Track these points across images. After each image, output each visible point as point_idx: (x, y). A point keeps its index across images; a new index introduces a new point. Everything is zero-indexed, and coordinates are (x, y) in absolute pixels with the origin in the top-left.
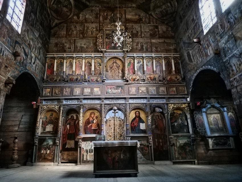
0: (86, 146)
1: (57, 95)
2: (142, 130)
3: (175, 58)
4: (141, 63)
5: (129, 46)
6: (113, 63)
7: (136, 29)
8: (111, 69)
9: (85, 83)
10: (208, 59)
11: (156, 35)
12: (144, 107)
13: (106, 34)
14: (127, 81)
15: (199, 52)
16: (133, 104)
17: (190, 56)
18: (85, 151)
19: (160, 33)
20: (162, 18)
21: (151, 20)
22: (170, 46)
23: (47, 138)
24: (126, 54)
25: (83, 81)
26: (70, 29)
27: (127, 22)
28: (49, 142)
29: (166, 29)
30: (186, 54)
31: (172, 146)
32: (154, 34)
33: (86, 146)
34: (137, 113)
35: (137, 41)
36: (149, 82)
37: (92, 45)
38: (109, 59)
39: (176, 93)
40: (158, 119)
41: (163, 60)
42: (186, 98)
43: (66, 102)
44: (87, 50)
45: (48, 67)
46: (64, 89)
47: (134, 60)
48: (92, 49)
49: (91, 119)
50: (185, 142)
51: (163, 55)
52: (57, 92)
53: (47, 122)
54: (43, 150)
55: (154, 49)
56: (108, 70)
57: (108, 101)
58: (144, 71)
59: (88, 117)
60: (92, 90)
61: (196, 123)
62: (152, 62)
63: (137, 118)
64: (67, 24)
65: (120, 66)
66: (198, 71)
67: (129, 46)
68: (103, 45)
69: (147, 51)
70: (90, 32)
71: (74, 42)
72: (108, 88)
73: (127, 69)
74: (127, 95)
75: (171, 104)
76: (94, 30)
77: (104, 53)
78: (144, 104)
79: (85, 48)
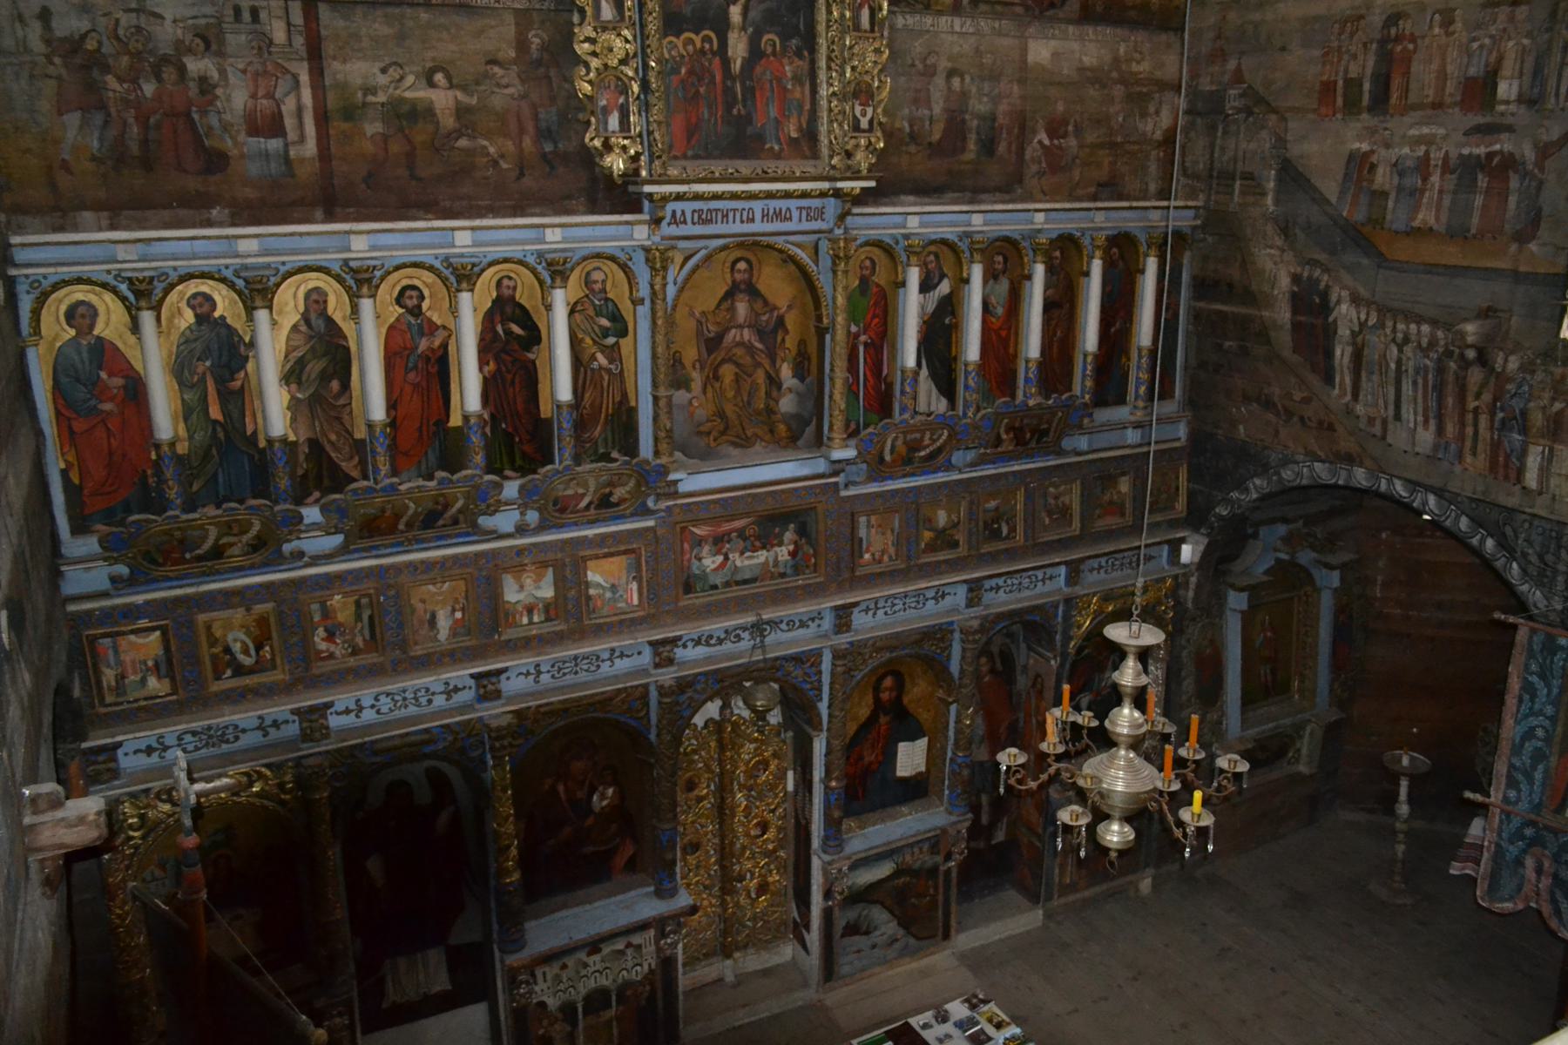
1: (247, 681)
4: (945, 287)
5: (864, 124)
6: (730, 295)
17: (1330, 332)
30: (1285, 282)
33: (562, 987)
44: (463, 143)
48: (522, 131)
63: (883, 719)
65: (781, 322)
67: (871, 122)
71: (299, 41)
72: (700, 542)
79: (448, 122)
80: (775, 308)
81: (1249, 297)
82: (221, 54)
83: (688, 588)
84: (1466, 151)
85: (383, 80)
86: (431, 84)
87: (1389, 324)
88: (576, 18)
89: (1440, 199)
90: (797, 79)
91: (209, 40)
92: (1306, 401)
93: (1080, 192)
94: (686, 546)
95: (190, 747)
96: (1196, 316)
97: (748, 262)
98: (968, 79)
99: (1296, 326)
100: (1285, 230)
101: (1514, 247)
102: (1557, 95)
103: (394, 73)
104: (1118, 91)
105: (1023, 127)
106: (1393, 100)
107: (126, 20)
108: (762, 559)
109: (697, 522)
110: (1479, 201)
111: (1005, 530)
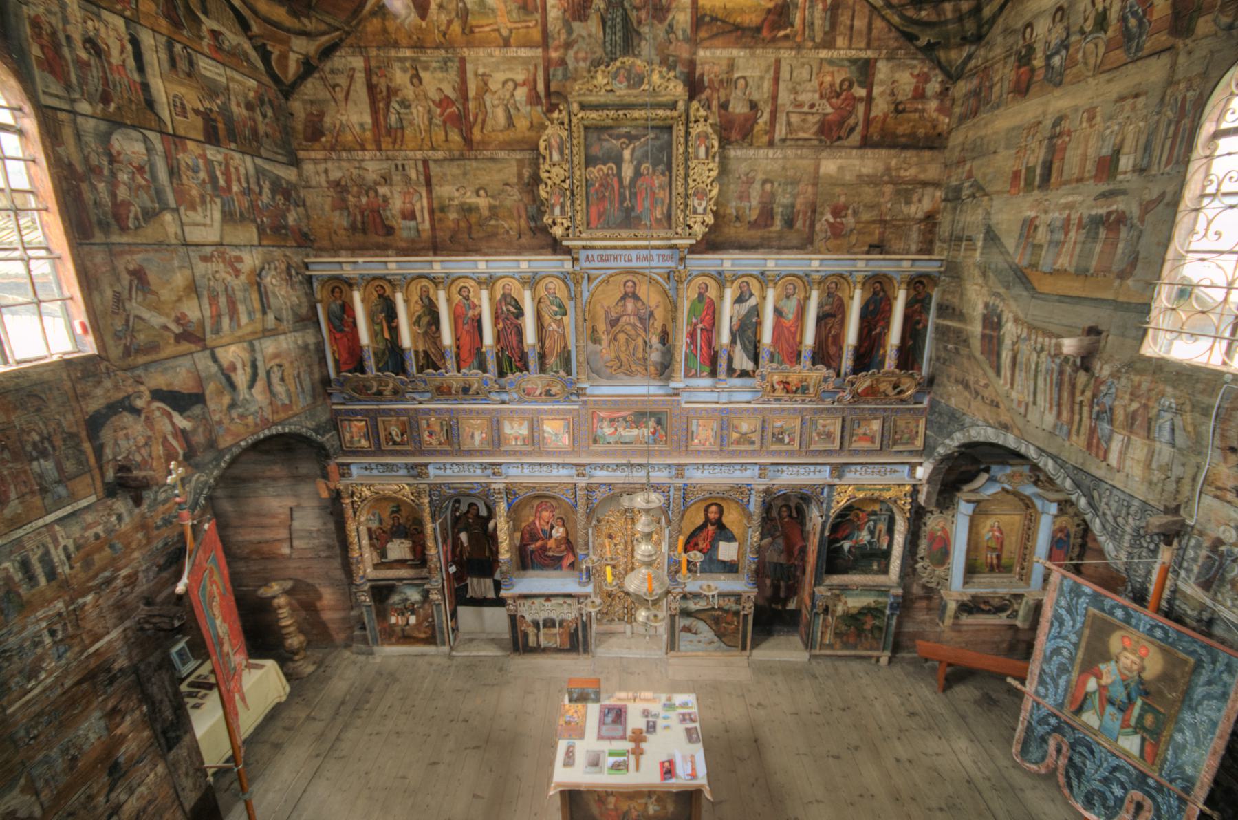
1: (398, 448)
2: (723, 562)
4: (753, 301)
5: (700, 210)
6: (623, 298)
7: (747, 84)
8: (612, 327)
11: (852, 130)
13: (586, 128)
17: (1000, 341)
19: (872, 115)
20: (910, 13)
21: (844, 19)
26: (388, 96)
27: (703, 34)
29: (916, 88)
30: (980, 309)
32: (841, 123)
35: (744, 167)
39: (877, 446)
42: (913, 467)
44: (493, 222)
45: (329, 320)
48: (520, 217)
60: (534, 426)
62: (802, 295)
63: (710, 528)
64: (360, 49)
65: (651, 314)
67: (705, 209)
68: (573, 203)
70: (500, 113)
71: (422, 178)
72: (602, 420)
76: (521, 94)
79: (486, 213)
81: (961, 317)
82: (391, 185)
83: (595, 441)
84: (1093, 212)
85: (457, 194)
86: (478, 195)
87: (1033, 337)
88: (541, 160)
89: (1074, 248)
90: (661, 187)
91: (386, 179)
92: (986, 386)
93: (856, 250)
96: (937, 328)
98: (776, 184)
99: (984, 336)
100: (984, 275)
101: (1117, 283)
102: (1159, 163)
103: (462, 191)
104: (888, 189)
105: (814, 211)
106: (1053, 180)
107: (355, 172)
109: (602, 410)
110: (1098, 248)
111: (787, 440)
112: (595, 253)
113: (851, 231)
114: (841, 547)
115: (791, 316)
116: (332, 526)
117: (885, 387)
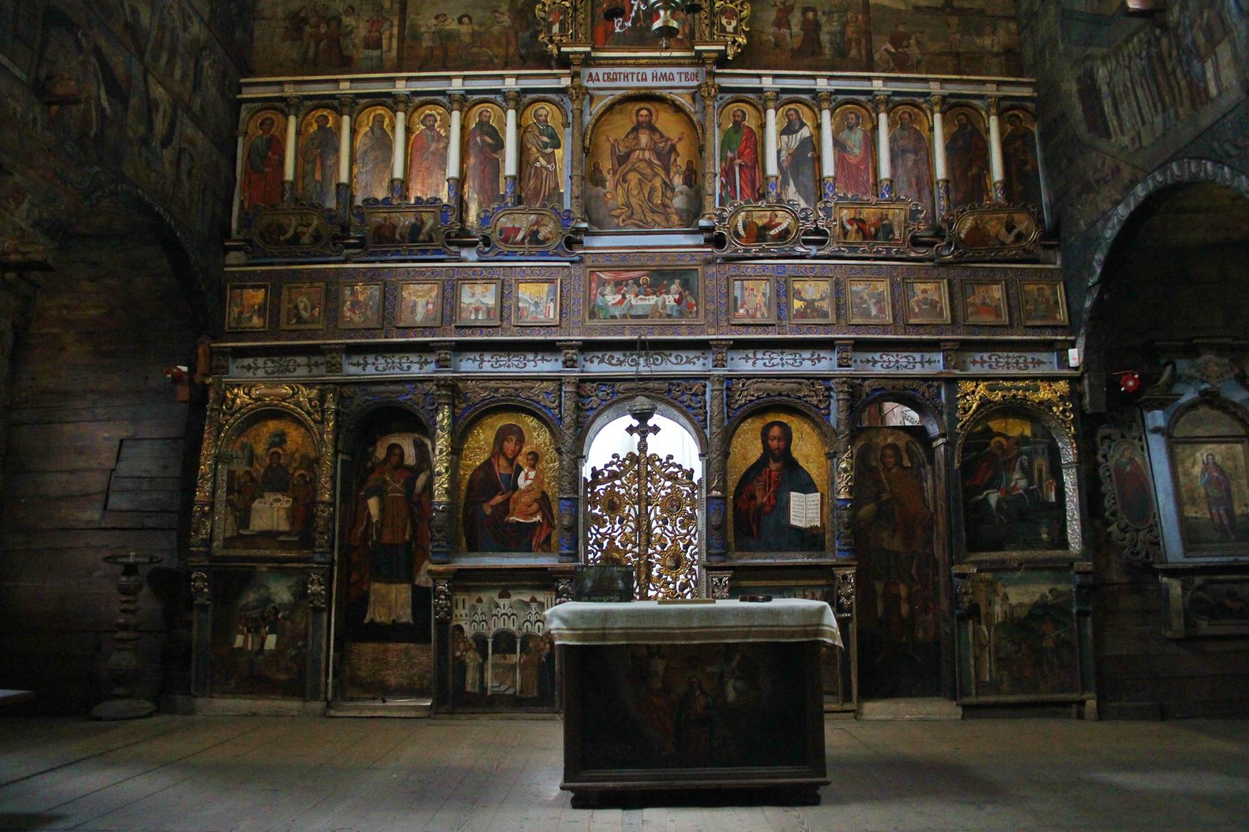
0: (477, 618)
1: (302, 327)
3: (1007, 109)
4: (805, 132)
5: (730, 29)
6: (635, 130)
8: (620, 165)
9: (464, 253)
10: (1206, 119)
12: (814, 401)
14: (719, 242)
15: (1154, 74)
16: (748, 378)
18: (471, 641)
22: (980, 34)
23: (263, 568)
24: (716, 75)
25: (451, 244)
28: (273, 590)
30: (1074, 87)
31: (963, 619)
33: (477, 618)
34: (776, 431)
36: (852, 249)
37: (506, 20)
38: (610, 109)
39: (1005, 319)
40: (894, 471)
41: (937, 117)
42: (1061, 350)
43: (358, 364)
45: (249, 158)
46: (347, 292)
47: (762, 113)
48: (509, 43)
49: (502, 468)
50: (1037, 597)
51: (934, 88)
52: (301, 306)
53: (253, 480)
54: (242, 633)
55: (884, 47)
56: (605, 173)
57: (602, 361)
58: (820, 181)
59: (486, 456)
61: (1104, 496)
62: (869, 126)
63: (773, 466)
65: (673, 148)
66: (1140, 192)
67: (735, 28)
68: (574, 18)
69: (840, 60)
72: (604, 283)
73: (718, 170)
74: (717, 325)
75: (976, 379)
77: (577, 69)
78: (817, 379)
79: (467, 39)
80: (668, 139)
83: (593, 315)
92: (1103, 164)
94: (593, 285)
95: (269, 370)
97: (648, 110)
98: (820, 13)
108: (652, 302)
109: (604, 269)
112: (601, 71)
113: (919, 62)
114: (986, 500)
115: (857, 151)
116: (176, 471)
117: (994, 226)
